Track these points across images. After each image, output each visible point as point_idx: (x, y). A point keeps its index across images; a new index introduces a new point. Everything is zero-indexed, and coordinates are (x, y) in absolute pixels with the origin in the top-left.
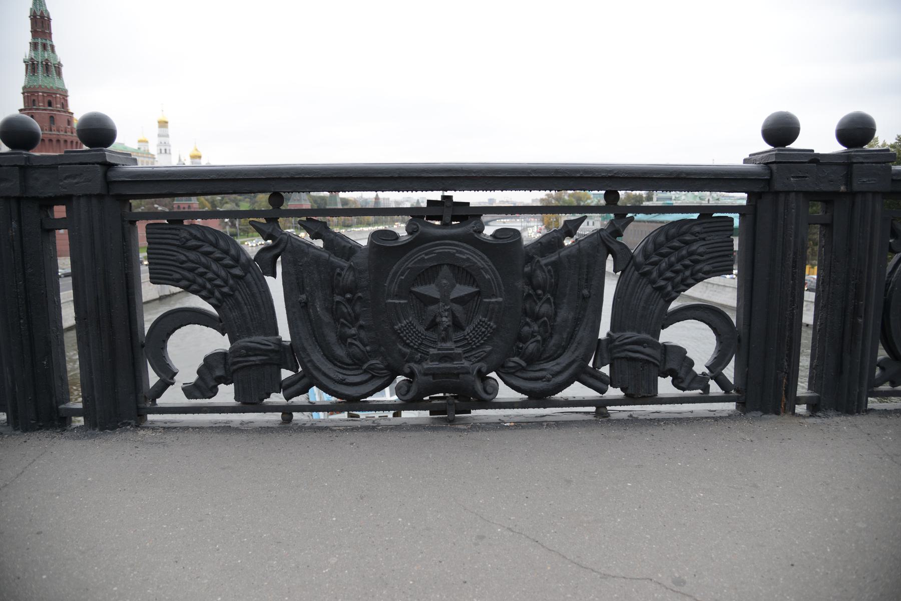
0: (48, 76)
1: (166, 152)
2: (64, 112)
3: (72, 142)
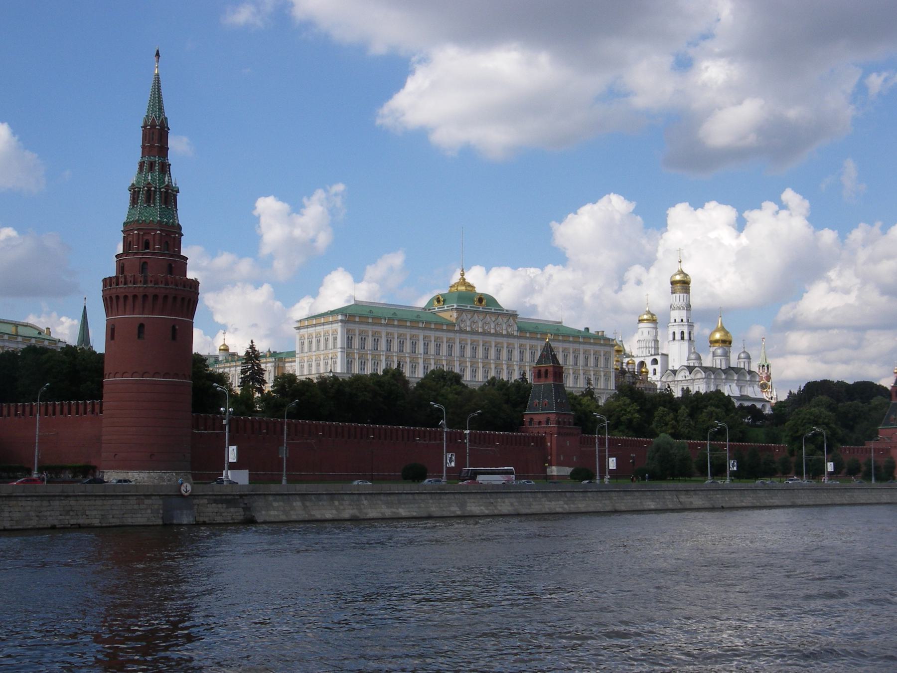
0: (150, 206)
1: (683, 338)
2: (172, 256)
3: (166, 297)
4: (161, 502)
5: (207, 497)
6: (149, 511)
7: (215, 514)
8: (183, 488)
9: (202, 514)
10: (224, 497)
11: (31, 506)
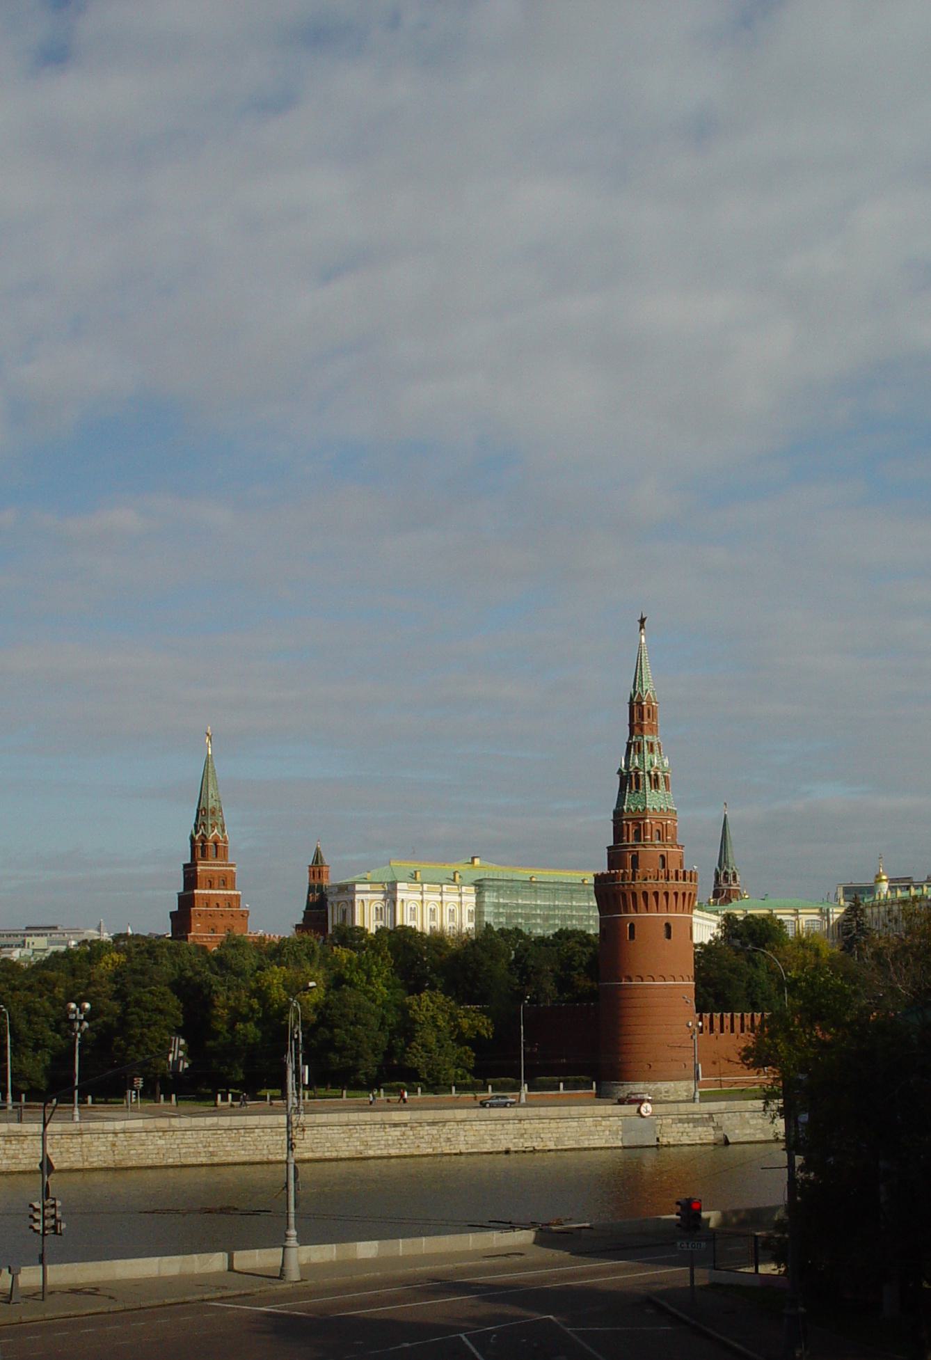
4: (620, 1123)
5: (673, 1117)
6: (607, 1133)
7: (680, 1134)
8: (643, 1110)
9: (665, 1135)
10: (691, 1116)
11: (486, 1131)
